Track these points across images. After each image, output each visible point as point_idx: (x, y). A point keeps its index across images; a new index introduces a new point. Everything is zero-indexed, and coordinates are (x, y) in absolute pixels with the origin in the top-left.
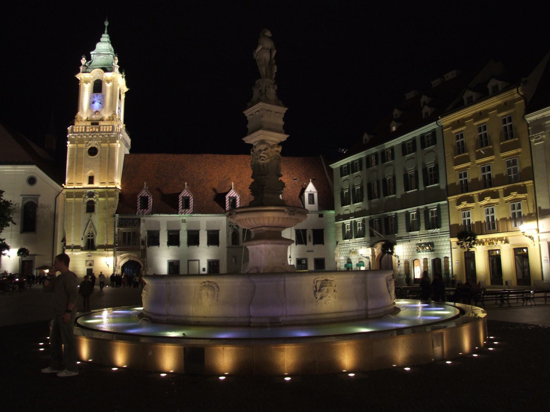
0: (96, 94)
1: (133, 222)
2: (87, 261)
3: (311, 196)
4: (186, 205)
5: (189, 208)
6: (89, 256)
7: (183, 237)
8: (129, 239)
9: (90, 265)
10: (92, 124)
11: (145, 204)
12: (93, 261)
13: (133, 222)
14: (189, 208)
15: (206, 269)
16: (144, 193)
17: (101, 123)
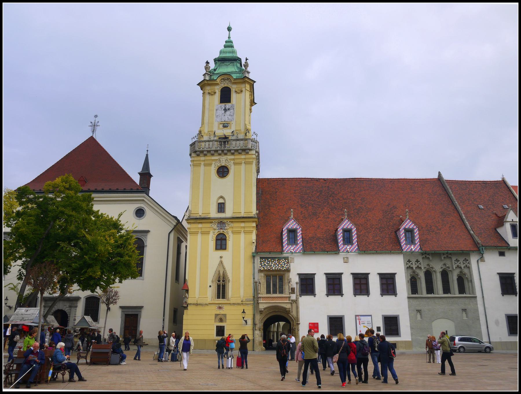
0: (223, 104)
1: (279, 262)
2: (216, 315)
3: (513, 227)
4: (348, 240)
5: (352, 244)
6: (220, 308)
7: (347, 284)
8: (275, 285)
9: (221, 320)
10: (219, 138)
11: (293, 240)
12: (225, 315)
13: (279, 262)
14: (352, 244)
15: (382, 329)
16: (292, 224)
17: (230, 138)
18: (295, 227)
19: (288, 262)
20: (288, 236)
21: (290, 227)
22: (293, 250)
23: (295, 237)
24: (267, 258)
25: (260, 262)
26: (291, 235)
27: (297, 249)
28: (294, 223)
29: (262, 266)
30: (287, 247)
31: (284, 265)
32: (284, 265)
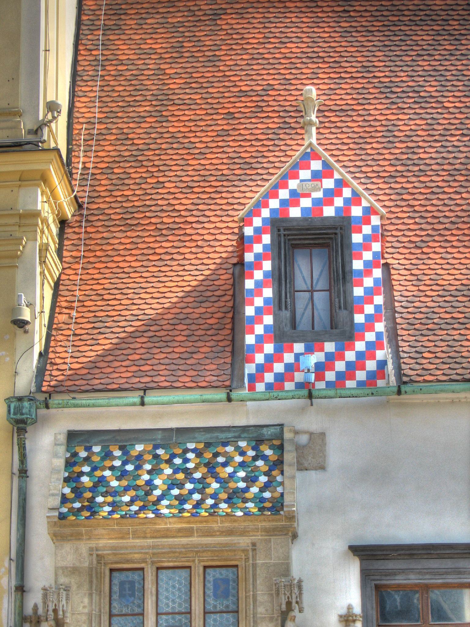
1: (211, 467)
13: (211, 467)
18: (329, 212)
19: (278, 464)
20: (282, 278)
21: (295, 213)
22: (320, 370)
23: (340, 278)
24: (124, 438)
25: (69, 464)
26: (309, 270)
27: (352, 368)
28: (329, 183)
29: (78, 492)
30: (277, 357)
31: (251, 480)
32: (251, 480)
